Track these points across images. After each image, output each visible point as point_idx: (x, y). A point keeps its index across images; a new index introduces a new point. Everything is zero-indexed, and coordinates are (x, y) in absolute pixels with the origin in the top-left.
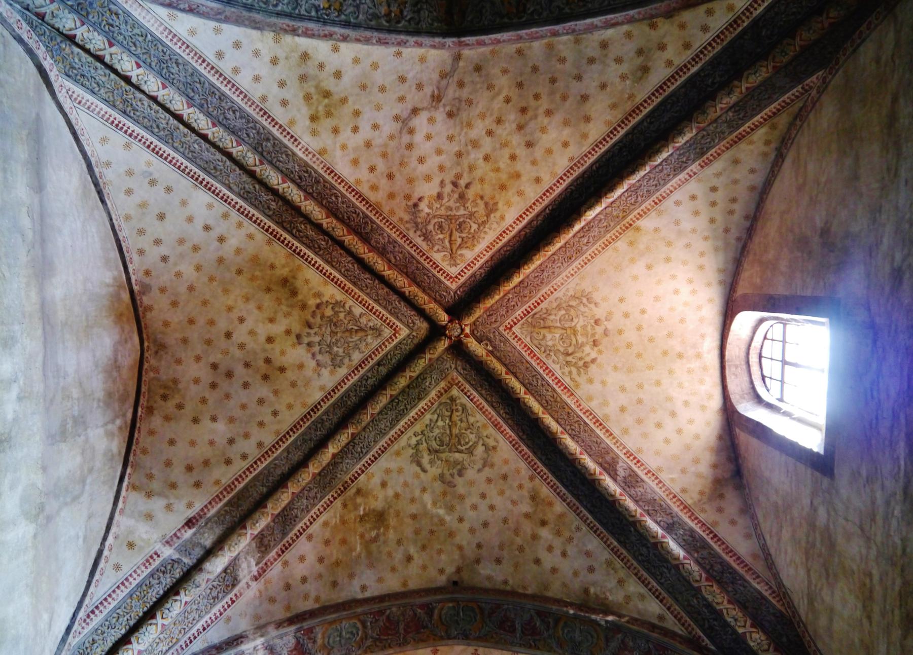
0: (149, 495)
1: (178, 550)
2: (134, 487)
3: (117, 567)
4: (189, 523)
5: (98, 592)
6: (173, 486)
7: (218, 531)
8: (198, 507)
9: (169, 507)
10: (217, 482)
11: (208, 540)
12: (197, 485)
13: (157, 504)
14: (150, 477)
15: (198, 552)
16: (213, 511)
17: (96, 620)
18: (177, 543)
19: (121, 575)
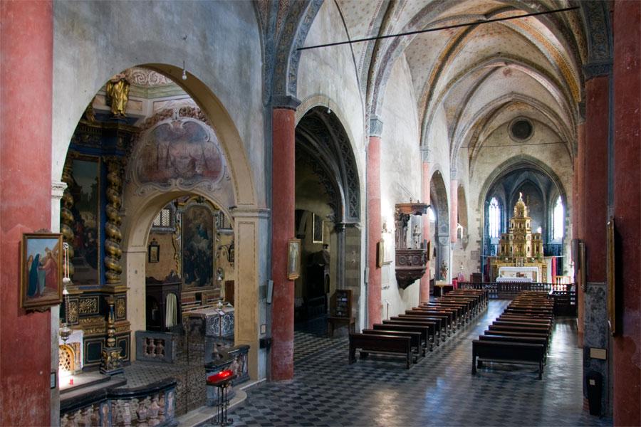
0: (355, 26)
1: (372, 34)
2: (350, 27)
3: (358, 52)
4: (371, 25)
5: (358, 60)
6: (361, 18)
7: (381, 20)
8: (371, 18)
9: (363, 25)
10: (374, 7)
11: (379, 25)
12: (368, 13)
13: (359, 26)
14: (353, 21)
15: (378, 30)
16: (377, 15)
17: (361, 70)
18: (370, 33)
19: (360, 54)
